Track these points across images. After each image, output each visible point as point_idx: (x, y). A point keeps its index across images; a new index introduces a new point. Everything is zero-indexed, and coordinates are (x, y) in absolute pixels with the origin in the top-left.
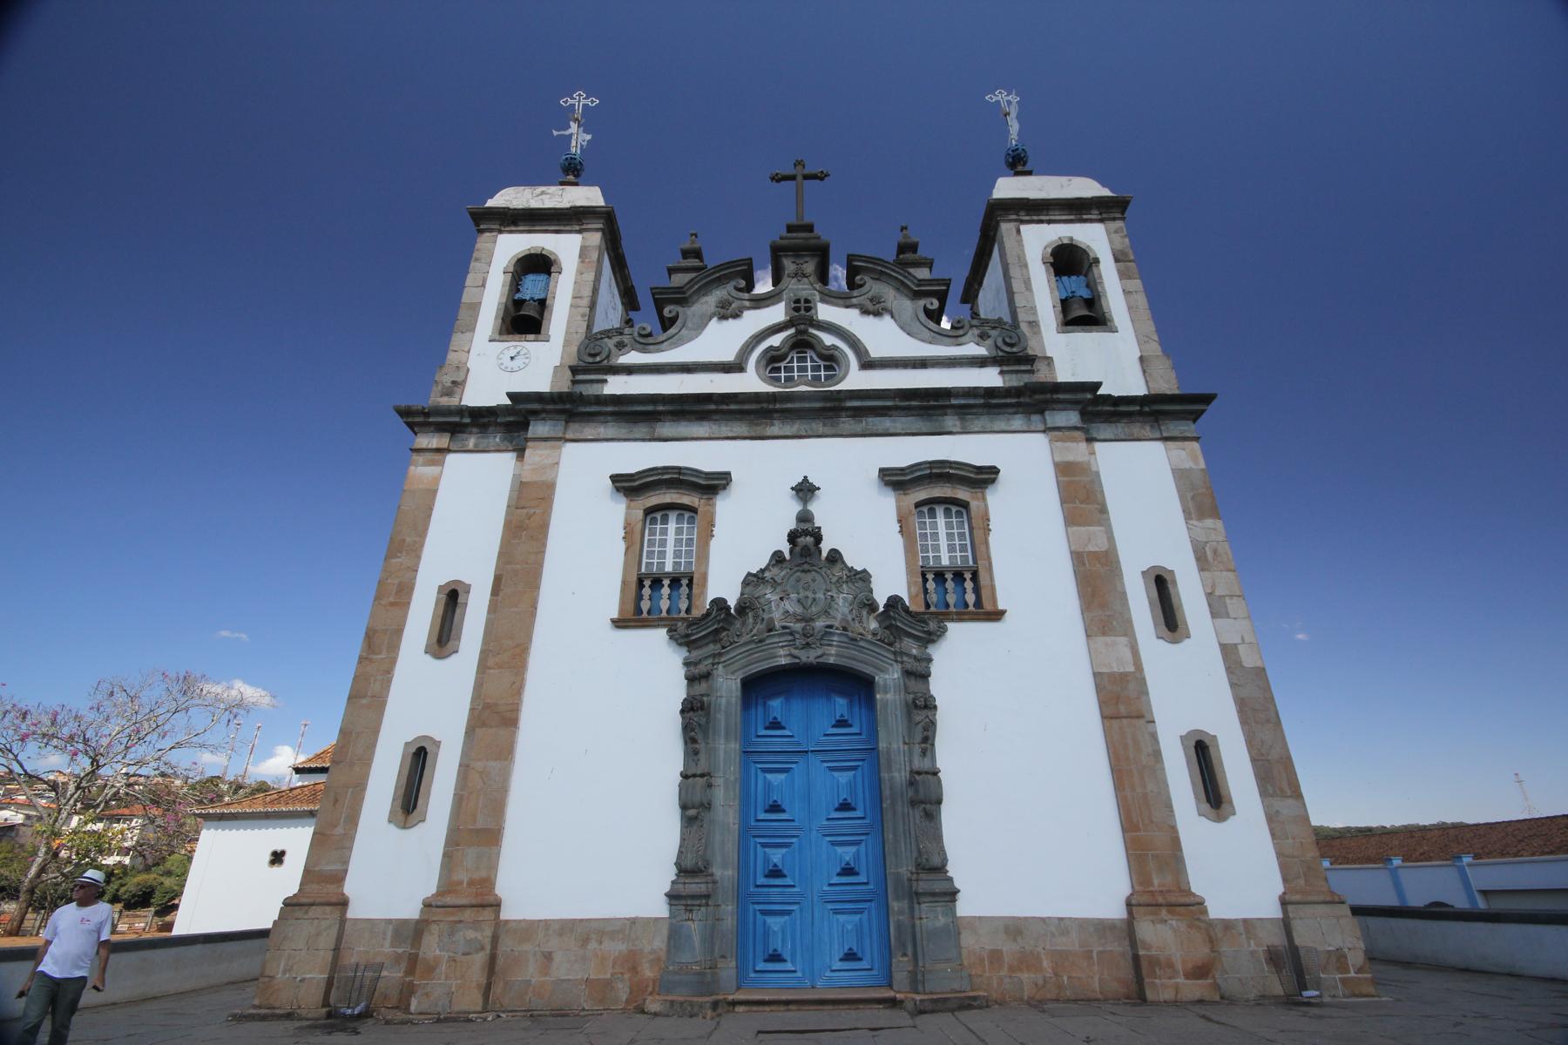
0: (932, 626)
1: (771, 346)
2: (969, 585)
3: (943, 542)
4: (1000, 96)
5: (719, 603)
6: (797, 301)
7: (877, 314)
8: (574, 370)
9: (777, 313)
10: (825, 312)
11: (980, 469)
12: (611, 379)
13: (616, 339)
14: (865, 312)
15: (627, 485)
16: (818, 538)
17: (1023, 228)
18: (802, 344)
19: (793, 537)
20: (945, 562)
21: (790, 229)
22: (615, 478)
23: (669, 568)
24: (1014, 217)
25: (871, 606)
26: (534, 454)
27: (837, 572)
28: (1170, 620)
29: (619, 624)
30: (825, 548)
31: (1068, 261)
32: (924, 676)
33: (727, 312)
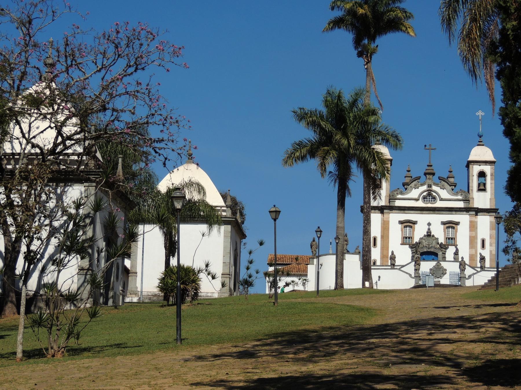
0: (447, 247)
1: (424, 195)
2: (453, 240)
3: (450, 233)
4: (480, 113)
5: (416, 242)
6: (429, 185)
7: (443, 189)
8: (390, 199)
9: (425, 188)
10: (434, 188)
11: (457, 222)
12: (396, 201)
13: (396, 192)
14: (441, 188)
15: (401, 222)
16: (431, 233)
17: (474, 166)
18: (429, 194)
19: (427, 233)
20: (450, 236)
21: (428, 166)
22: (399, 221)
23: (408, 236)
24: (472, 164)
25: (438, 243)
26: (386, 215)
27: (434, 238)
28: (483, 246)
29: (402, 244)
30: (432, 234)
31: (482, 174)
32: (445, 254)
33: (416, 187)
